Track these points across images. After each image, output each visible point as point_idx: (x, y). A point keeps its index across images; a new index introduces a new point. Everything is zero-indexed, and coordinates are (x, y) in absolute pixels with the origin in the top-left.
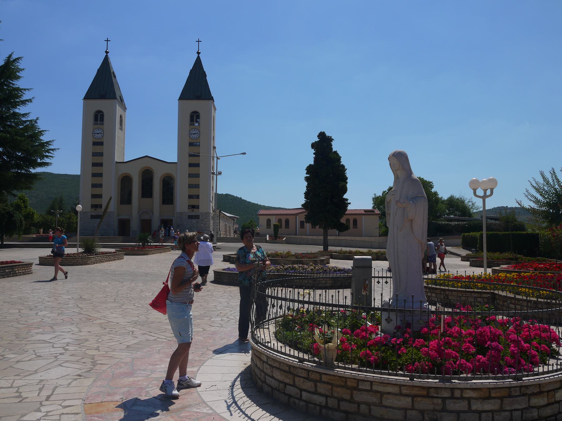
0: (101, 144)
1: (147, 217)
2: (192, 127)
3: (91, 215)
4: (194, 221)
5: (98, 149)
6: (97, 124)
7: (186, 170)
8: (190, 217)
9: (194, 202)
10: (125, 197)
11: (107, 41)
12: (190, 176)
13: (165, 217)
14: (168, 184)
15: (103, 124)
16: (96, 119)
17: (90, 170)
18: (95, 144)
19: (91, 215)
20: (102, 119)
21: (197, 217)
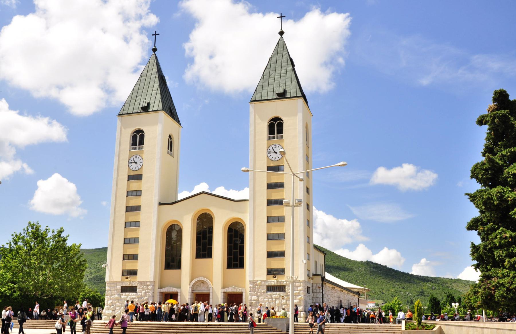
0: (139, 177)
1: (202, 290)
4: (276, 294)
5: (134, 185)
6: (135, 149)
7: (263, 211)
8: (271, 289)
9: (276, 263)
10: (172, 260)
11: (155, 35)
12: (270, 220)
13: (230, 290)
14: (236, 235)
17: (122, 216)
19: (122, 287)
20: (142, 143)
21: (281, 288)
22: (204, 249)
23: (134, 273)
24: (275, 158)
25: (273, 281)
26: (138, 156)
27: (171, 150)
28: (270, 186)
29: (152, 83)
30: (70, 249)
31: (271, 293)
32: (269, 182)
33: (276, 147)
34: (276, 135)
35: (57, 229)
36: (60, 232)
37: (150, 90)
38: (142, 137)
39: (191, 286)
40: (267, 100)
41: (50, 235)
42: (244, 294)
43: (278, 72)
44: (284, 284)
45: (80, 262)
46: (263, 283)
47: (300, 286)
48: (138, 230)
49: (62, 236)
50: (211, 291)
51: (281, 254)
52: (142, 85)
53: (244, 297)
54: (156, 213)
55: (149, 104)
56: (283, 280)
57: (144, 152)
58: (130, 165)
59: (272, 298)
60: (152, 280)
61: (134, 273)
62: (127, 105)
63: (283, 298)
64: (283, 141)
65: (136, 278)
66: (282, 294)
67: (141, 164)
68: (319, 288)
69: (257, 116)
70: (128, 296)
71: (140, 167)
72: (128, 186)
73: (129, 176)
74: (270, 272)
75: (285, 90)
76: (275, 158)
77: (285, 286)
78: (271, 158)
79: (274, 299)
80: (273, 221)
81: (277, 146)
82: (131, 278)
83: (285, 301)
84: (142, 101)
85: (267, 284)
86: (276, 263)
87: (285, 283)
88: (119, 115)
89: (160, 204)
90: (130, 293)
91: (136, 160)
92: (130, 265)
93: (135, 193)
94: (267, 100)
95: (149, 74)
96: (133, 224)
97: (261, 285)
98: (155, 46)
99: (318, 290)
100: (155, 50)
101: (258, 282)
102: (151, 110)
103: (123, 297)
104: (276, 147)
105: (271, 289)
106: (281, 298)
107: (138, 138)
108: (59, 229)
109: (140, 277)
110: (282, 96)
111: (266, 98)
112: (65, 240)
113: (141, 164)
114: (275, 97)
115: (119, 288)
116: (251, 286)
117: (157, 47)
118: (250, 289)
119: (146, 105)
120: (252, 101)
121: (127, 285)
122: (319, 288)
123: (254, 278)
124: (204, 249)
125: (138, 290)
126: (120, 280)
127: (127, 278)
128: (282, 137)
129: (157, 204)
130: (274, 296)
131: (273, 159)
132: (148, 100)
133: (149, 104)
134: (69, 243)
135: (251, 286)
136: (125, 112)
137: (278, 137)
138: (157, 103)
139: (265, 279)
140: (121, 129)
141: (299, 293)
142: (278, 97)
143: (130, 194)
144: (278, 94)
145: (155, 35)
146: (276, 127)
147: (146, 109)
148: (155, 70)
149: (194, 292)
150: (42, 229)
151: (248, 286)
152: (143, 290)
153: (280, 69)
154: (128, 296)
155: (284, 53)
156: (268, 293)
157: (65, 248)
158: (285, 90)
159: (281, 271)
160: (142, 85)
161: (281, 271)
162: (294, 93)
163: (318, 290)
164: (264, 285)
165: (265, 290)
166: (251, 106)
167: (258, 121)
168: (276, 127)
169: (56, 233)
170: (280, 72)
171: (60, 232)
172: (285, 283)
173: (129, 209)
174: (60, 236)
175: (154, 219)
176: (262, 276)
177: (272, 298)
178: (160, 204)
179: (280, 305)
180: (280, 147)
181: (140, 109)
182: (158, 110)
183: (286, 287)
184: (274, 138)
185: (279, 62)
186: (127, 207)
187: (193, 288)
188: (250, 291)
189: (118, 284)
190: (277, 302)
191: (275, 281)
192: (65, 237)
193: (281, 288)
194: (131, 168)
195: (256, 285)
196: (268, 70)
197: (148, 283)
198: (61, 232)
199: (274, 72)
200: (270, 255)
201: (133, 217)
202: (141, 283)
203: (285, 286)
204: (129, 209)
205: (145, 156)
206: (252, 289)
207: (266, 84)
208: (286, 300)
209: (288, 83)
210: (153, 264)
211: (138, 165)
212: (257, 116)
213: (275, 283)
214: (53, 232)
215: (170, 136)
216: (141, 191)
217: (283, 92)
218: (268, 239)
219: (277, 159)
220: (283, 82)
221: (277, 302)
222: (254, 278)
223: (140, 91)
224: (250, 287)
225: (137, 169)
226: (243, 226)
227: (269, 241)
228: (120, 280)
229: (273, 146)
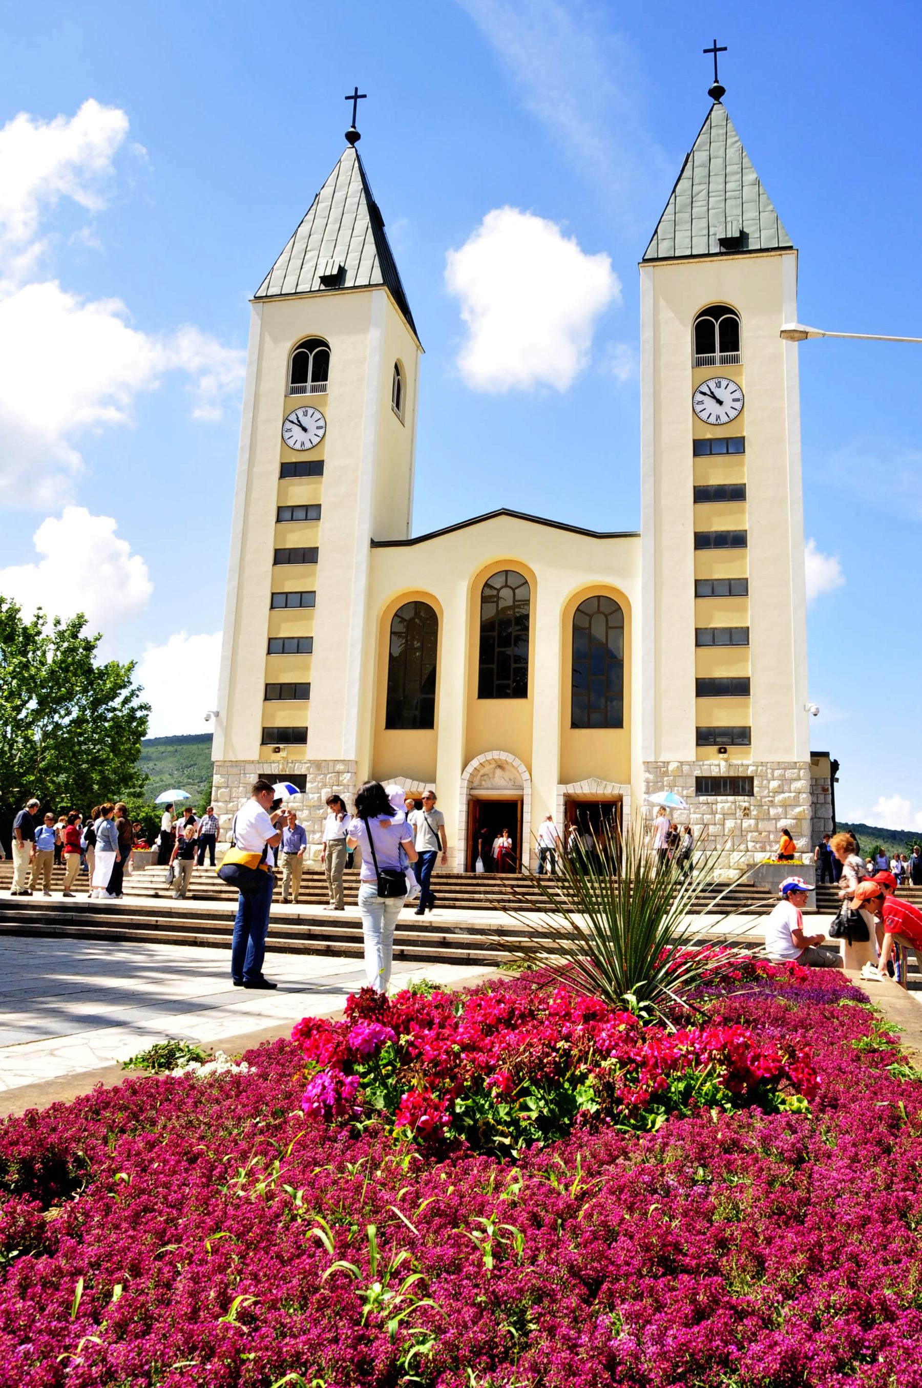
0: (314, 469)
2: (706, 371)
4: (724, 802)
5: (300, 492)
7: (685, 565)
8: (708, 786)
9: (724, 713)
10: (408, 700)
11: (356, 97)
12: (705, 589)
15: (324, 389)
16: (298, 374)
17: (263, 577)
18: (289, 470)
20: (321, 373)
21: (739, 785)
22: (502, 672)
23: (298, 736)
24: (718, 417)
25: (717, 765)
26: (310, 411)
27: (398, 405)
28: (702, 495)
29: (348, 219)
30: (102, 674)
31: (711, 799)
32: (702, 483)
33: (718, 385)
34: (718, 354)
35: (68, 618)
36: (78, 625)
37: (345, 233)
38: (323, 360)
39: (467, 775)
40: (692, 256)
41: (48, 631)
42: (626, 801)
43: (717, 184)
44: (749, 773)
45: (133, 710)
46: (686, 768)
47: (798, 779)
48: (310, 618)
49: (81, 636)
50: (527, 791)
51: (739, 688)
52: (320, 222)
53: (626, 810)
54: (364, 567)
55: (342, 271)
56: (745, 762)
57: (330, 398)
58: (287, 435)
59: (714, 813)
60: (352, 756)
61: (298, 736)
62: (278, 273)
63: (746, 812)
64: (740, 374)
65: (304, 753)
66: (743, 801)
67: (321, 432)
68: (825, 790)
69: (662, 302)
71: (316, 440)
72: (281, 493)
73: (283, 465)
74: (705, 737)
75: (742, 232)
76: (718, 417)
77: (751, 779)
78: (704, 415)
79: (718, 816)
80: (713, 594)
81: (724, 383)
82: (289, 751)
83: (752, 822)
84: (322, 262)
85: (698, 773)
86: (724, 713)
87: (751, 769)
88: (257, 298)
89: (375, 544)
91: (305, 421)
92: (286, 715)
93: (301, 514)
94: (692, 256)
95: (339, 195)
96: (294, 599)
97: (679, 773)
98: (354, 126)
99: (821, 797)
100: (353, 137)
101: (671, 767)
102: (349, 283)
104: (718, 385)
105: (708, 786)
106: (739, 814)
107: (310, 363)
108: (73, 617)
109: (313, 749)
110: (735, 245)
111: (688, 253)
112: (89, 647)
113: (321, 432)
114: (715, 249)
116: (651, 777)
117: (359, 129)
118: (648, 787)
119: (335, 272)
120: (645, 261)
122: (825, 790)
123: (657, 753)
124: (502, 672)
125: (308, 785)
126: (255, 756)
127: (277, 750)
128: (736, 360)
129: (367, 543)
130: (719, 806)
131: (712, 420)
132: (339, 260)
133: (342, 271)
134: (98, 661)
135: (651, 777)
136: (273, 291)
137: (724, 361)
138: (364, 268)
139: (691, 757)
140: (262, 335)
141: (797, 798)
142: (723, 250)
143: (288, 515)
144: (723, 242)
145: (356, 97)
146: (717, 332)
147: (334, 281)
148: (357, 185)
149: (475, 792)
150: (26, 618)
151: (640, 776)
152: (324, 786)
153: (722, 180)
155: (730, 141)
156: (704, 798)
157: (90, 670)
158: (742, 232)
159: (741, 736)
160: (320, 222)
161: (741, 736)
162: (770, 238)
163: (821, 797)
164: (688, 776)
165: (693, 789)
166: (646, 272)
167: (666, 314)
168: (717, 332)
169: (63, 627)
170: (722, 187)
171: (78, 625)
172: (751, 769)
173: (282, 557)
174: (75, 636)
175: (358, 585)
176: (683, 749)
177: (714, 813)
178: (375, 544)
179: (738, 833)
180: (732, 387)
181: (317, 281)
182: (369, 285)
183: (756, 783)
184: (712, 362)
185: (717, 163)
186: (277, 551)
187: (470, 781)
189: (252, 767)
190: (730, 824)
191: (723, 763)
192: (91, 639)
193: (739, 785)
194: (291, 442)
195: (666, 773)
196: (684, 184)
197: (340, 767)
198: (80, 625)
199: (705, 186)
200: (706, 688)
201: (295, 579)
202: (318, 765)
203: (751, 779)
204: (282, 557)
205: (329, 412)
207: (686, 216)
208: (757, 819)
209: (751, 214)
210: (355, 711)
211: (310, 435)
212: (662, 302)
214: (58, 622)
215: (396, 367)
216: (319, 506)
217: (737, 235)
218: (698, 645)
219: (724, 419)
220: (733, 210)
221: (730, 824)
222: (657, 753)
223: (316, 237)
224: (648, 782)
225: (308, 445)
226: (619, 608)
227: (703, 650)
228: (255, 756)
229: (712, 384)
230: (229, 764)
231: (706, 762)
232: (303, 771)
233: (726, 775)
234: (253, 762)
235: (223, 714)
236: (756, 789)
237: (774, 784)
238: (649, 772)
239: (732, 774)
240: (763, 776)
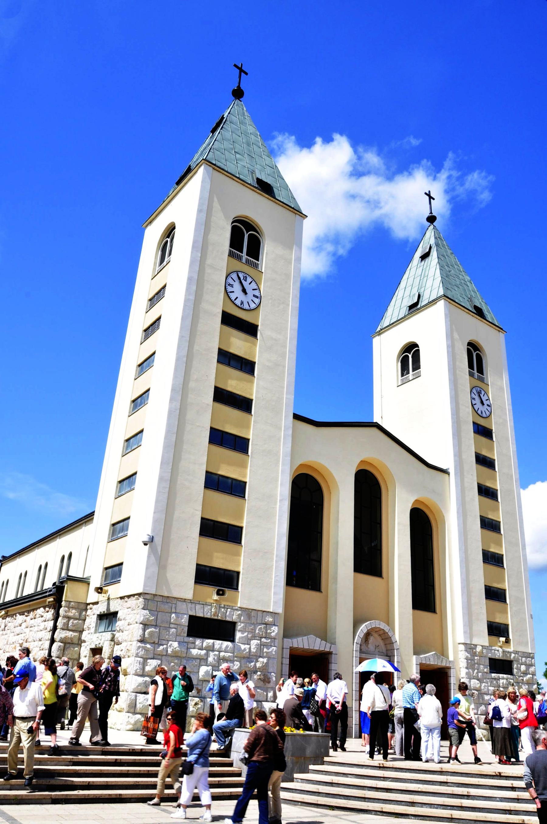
3: (193, 619)
70: (211, 649)
85: (490, 655)
90: (218, 643)
97: (481, 655)
101: (479, 649)
103: (195, 652)
115: (185, 620)
121: (208, 616)
125: (238, 635)
139: (487, 644)
152: (254, 637)
154: (211, 649)
156: (493, 675)
172: (513, 655)
188: (466, 668)
197: (270, 619)
202: (248, 612)
206: (471, 665)
213: (501, 655)
224: (467, 659)
230: (160, 599)
231: (493, 648)
232: (234, 618)
233: (502, 658)
234: (184, 600)
235: (158, 540)
236: (515, 671)
237: (523, 668)
238: (466, 651)
239: (505, 658)
240: (517, 661)
